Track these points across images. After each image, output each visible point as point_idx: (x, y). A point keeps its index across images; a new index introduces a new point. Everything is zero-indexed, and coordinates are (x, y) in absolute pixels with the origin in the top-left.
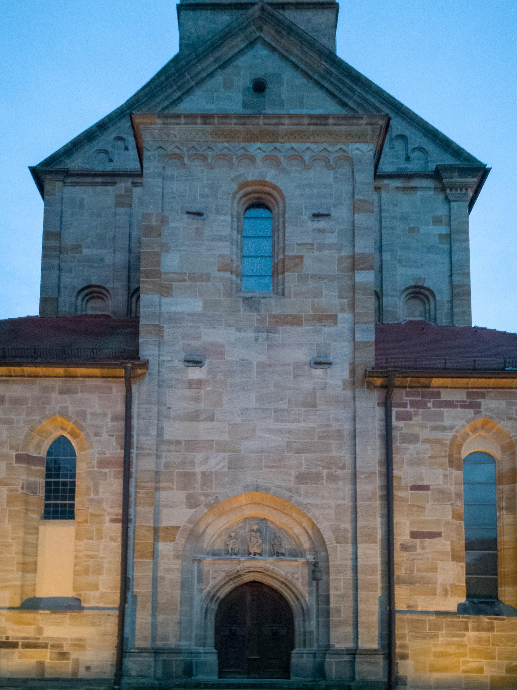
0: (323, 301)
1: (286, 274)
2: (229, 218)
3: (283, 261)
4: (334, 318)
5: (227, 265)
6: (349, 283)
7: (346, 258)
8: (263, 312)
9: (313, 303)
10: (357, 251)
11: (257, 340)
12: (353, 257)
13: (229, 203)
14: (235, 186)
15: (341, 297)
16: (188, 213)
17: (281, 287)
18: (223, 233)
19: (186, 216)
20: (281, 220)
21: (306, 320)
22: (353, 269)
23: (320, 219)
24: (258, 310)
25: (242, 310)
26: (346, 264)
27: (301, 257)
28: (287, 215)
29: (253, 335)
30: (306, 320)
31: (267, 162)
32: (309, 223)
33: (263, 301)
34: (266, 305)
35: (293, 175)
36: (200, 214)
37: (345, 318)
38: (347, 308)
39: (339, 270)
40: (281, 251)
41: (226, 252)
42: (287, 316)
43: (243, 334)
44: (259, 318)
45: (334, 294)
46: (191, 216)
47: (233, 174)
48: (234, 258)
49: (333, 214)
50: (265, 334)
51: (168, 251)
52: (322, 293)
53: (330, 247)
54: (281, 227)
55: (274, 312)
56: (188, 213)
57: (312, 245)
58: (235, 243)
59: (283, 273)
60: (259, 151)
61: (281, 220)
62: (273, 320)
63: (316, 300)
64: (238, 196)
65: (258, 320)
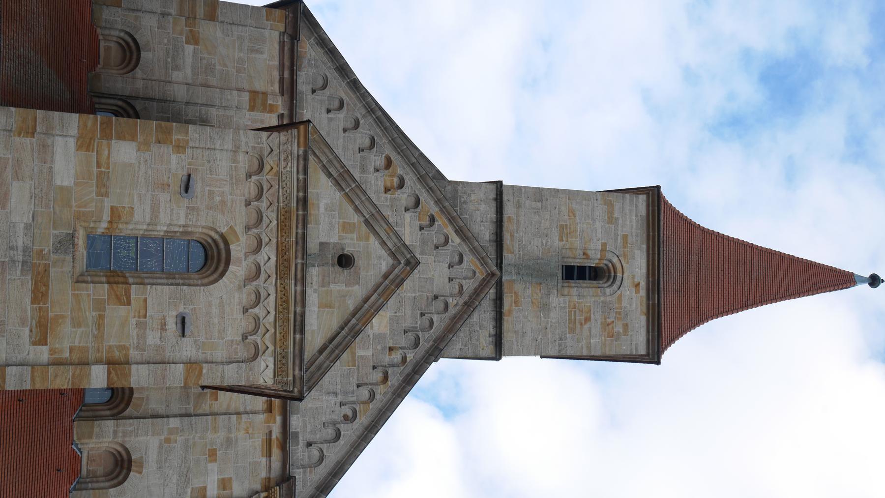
0: (67, 328)
1: (106, 286)
2: (182, 222)
3: (127, 283)
4: (43, 341)
5: (119, 217)
6: (92, 356)
7: (127, 356)
8: (53, 257)
9: (63, 317)
10: (134, 367)
11: (12, 248)
12: (127, 363)
13: (202, 222)
14: (224, 230)
15: (71, 350)
16: (189, 176)
17: (89, 279)
18: (162, 215)
19: (185, 173)
20: (181, 282)
21: (40, 308)
22: (111, 363)
23: (179, 325)
24: (56, 251)
25: (55, 232)
26: (117, 354)
27: (129, 304)
28: (185, 287)
29: (20, 244)
30: (40, 308)
31: (253, 267)
32: (175, 313)
33: (69, 258)
34: (64, 260)
35: (237, 295)
36: (187, 191)
37: (43, 354)
38: (56, 356)
39: (110, 347)
40: (138, 280)
41: (137, 217)
42: (47, 285)
43: (21, 233)
44: (45, 252)
45: (77, 341)
46: (185, 179)
47: (239, 229)
48: (131, 227)
49: (185, 339)
50: (20, 258)
51: (139, 150)
52: (79, 326)
53: (142, 337)
54: (171, 281)
55: (52, 270)
56: (189, 176)
57: (145, 317)
58: (150, 228)
59: (109, 283)
60: (266, 258)
61: (181, 282)
62: (41, 269)
63: (69, 321)
64: (213, 234)
65: (42, 251)
